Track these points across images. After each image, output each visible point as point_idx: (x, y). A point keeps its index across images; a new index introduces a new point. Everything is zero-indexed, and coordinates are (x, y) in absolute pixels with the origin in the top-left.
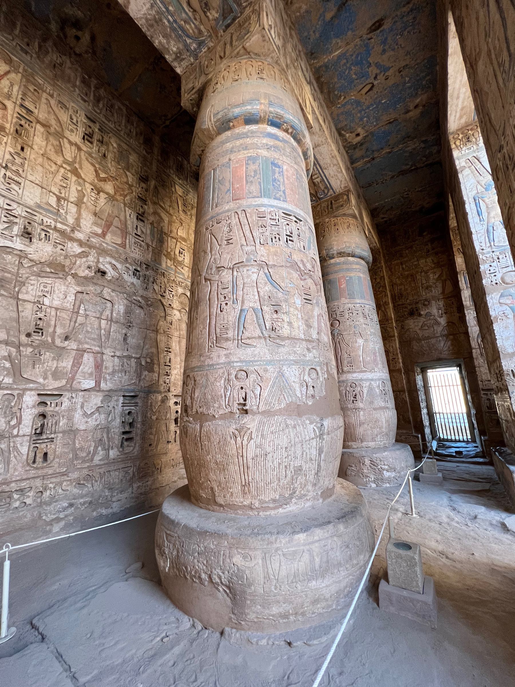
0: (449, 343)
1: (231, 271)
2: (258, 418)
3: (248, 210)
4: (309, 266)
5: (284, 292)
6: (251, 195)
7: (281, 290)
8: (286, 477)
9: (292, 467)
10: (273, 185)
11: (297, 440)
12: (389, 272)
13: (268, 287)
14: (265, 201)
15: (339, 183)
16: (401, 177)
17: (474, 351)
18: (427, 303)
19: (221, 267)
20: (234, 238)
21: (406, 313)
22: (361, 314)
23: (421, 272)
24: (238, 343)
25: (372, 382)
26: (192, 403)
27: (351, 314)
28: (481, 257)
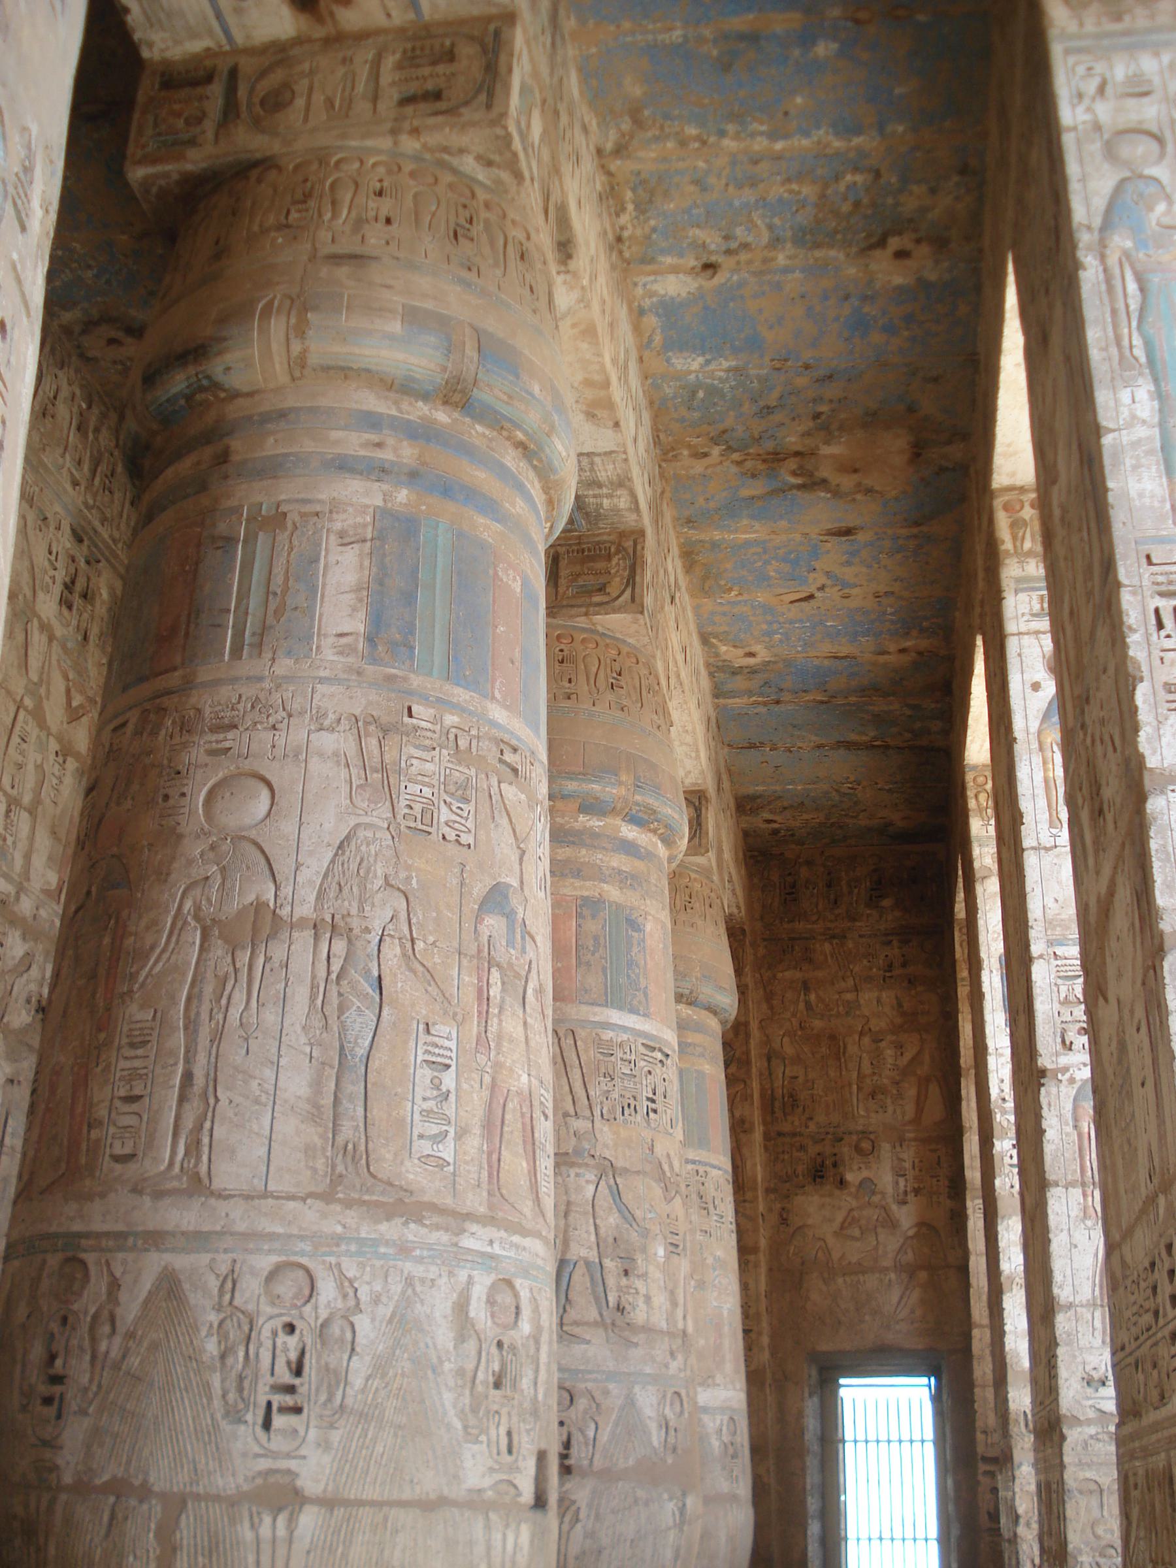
0: (915, 1295)
3: (581, 1033)
7: (634, 1224)
10: (629, 976)
12: (764, 1006)
14: (616, 1016)
16: (842, 751)
17: (976, 1332)
18: (866, 1148)
21: (800, 1169)
22: (694, 1196)
23: (861, 1034)
28: (998, 1116)
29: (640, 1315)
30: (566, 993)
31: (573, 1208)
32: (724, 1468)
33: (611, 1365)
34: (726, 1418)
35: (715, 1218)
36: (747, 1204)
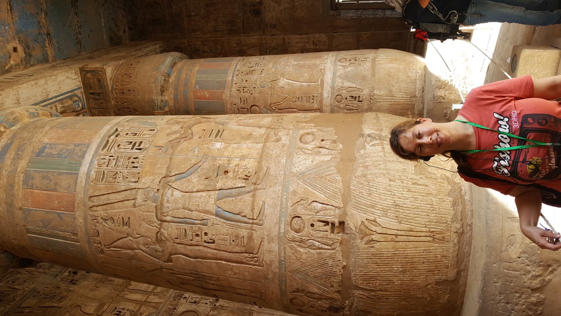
1: (165, 223)
2: (351, 210)
3: (91, 193)
4: (176, 127)
5: (204, 160)
6: (72, 187)
7: (200, 164)
8: (426, 186)
9: (415, 177)
10: (66, 157)
11: (381, 167)
13: (194, 179)
14: (84, 169)
15: (69, 80)
19: (157, 237)
20: (122, 215)
22: (247, 77)
24: (257, 224)
25: (338, 74)
26: (327, 299)
27: (246, 90)
29: (251, 164)
30: (70, 199)
31: (186, 206)
32: (360, 65)
33: (279, 188)
34: (339, 63)
35: (256, 67)
36: (267, 42)
